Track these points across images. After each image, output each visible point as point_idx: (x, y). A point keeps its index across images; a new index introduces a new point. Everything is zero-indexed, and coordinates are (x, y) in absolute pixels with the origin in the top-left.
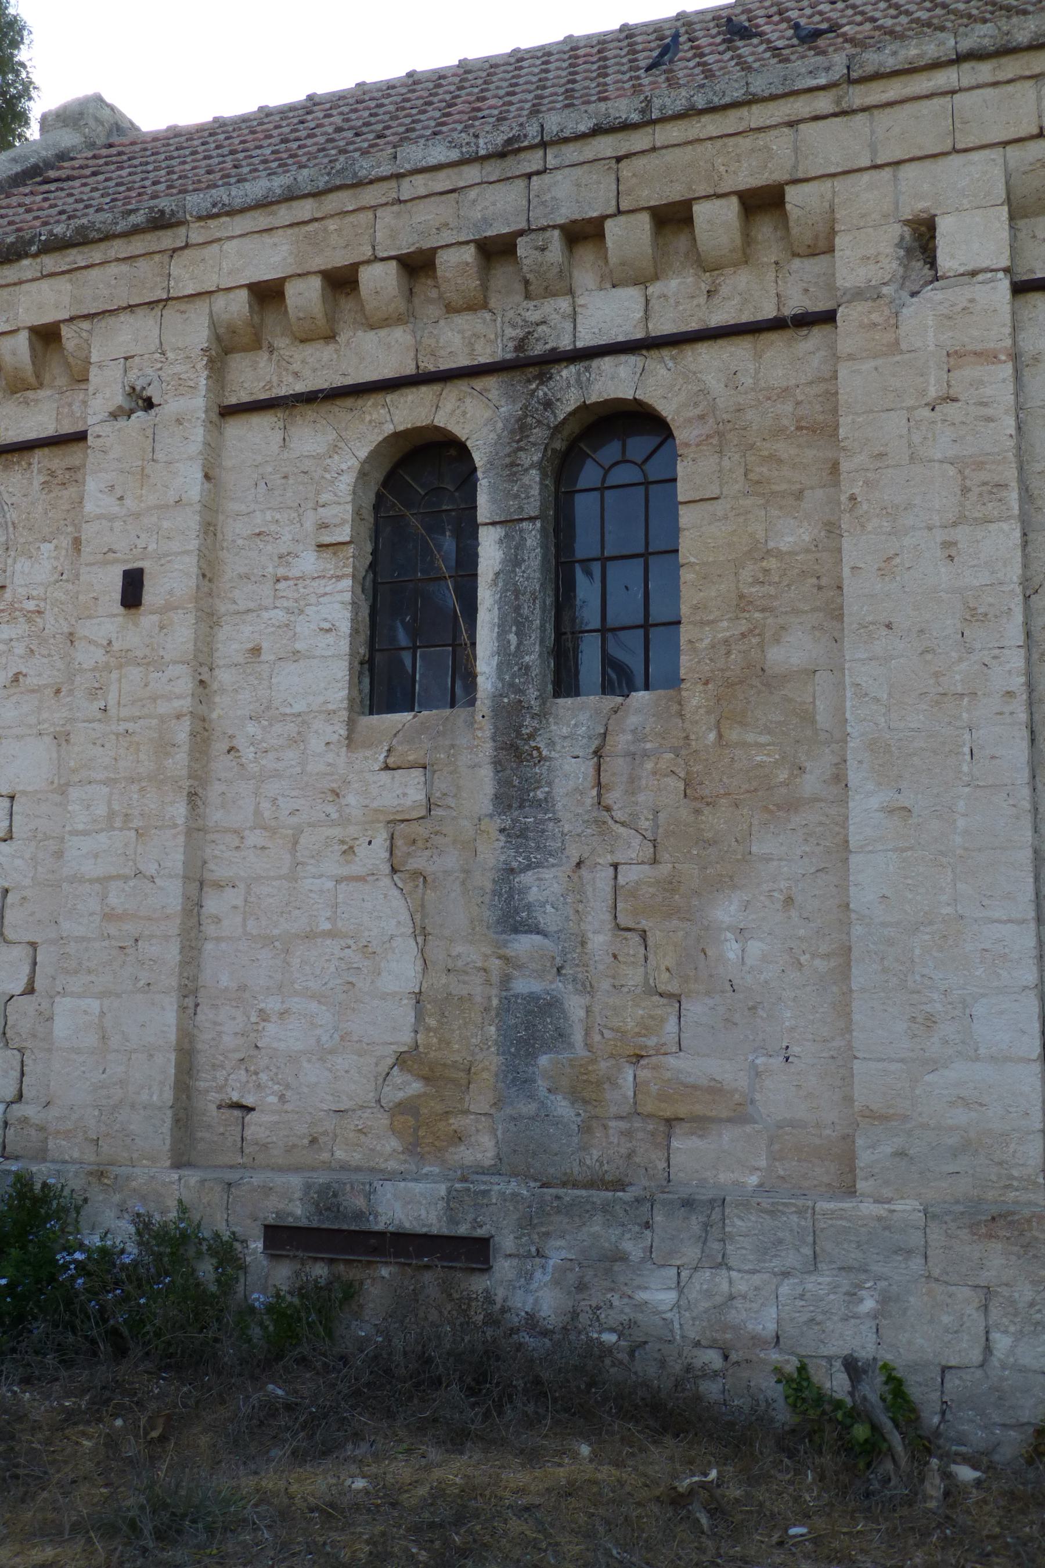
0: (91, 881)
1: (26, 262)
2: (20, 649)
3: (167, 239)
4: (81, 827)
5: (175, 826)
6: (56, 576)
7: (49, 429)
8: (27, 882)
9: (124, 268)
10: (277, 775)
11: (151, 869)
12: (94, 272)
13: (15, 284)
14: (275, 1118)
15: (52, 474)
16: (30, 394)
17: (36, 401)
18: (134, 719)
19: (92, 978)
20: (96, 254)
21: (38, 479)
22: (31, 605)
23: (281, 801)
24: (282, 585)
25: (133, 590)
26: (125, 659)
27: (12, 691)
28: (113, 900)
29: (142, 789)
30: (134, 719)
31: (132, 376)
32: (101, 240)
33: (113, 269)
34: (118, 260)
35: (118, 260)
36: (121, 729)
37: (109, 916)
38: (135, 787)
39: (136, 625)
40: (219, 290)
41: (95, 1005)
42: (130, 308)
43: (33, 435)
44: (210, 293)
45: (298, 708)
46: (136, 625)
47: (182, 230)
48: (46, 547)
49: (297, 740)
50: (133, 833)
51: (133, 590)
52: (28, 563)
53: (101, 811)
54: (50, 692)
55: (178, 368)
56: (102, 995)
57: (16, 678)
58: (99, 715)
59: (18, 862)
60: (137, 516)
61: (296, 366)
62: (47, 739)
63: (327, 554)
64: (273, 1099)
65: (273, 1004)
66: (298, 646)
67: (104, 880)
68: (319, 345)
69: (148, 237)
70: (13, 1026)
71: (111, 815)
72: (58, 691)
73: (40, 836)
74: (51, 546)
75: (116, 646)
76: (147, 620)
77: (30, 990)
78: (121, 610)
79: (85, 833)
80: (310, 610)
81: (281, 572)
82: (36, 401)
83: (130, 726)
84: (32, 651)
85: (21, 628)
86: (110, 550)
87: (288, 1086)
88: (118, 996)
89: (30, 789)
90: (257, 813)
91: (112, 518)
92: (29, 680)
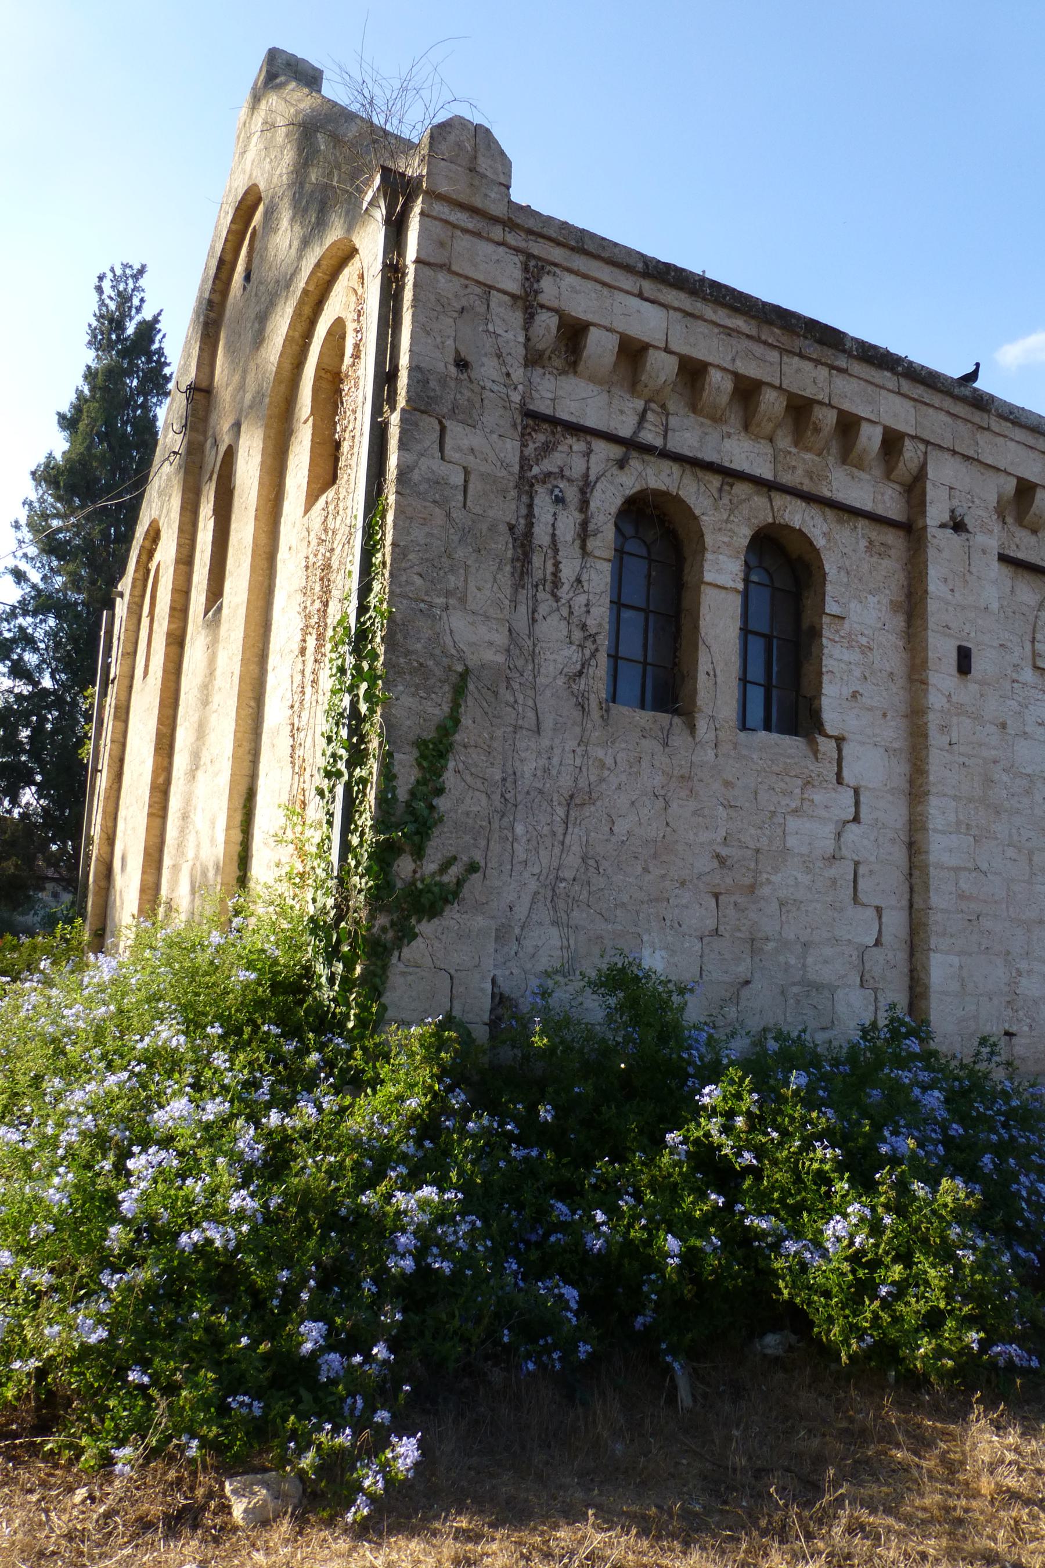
0: (952, 869)
1: (888, 374)
2: (857, 673)
3: (978, 417)
4: (940, 827)
5: (997, 839)
6: (880, 625)
7: (868, 507)
8: (873, 859)
9: (949, 420)
10: (1018, 812)
11: (984, 866)
12: (931, 410)
13: (877, 386)
14: (1028, 1041)
15: (871, 542)
16: (855, 470)
17: (860, 480)
18: (969, 756)
19: (953, 940)
20: (936, 399)
21: (863, 543)
22: (864, 641)
23: (1022, 830)
24: (1015, 685)
25: (964, 660)
26: (961, 710)
27: (853, 704)
28: (963, 885)
29: (976, 808)
30: (969, 756)
31: (956, 502)
32: (941, 391)
33: (943, 417)
34: (948, 412)
35: (948, 412)
36: (961, 760)
37: (962, 897)
38: (972, 806)
39: (966, 687)
40: (1005, 471)
41: (955, 960)
42: (954, 452)
43: (857, 505)
44: (998, 470)
45: (1029, 771)
46: (966, 687)
47: (986, 416)
48: (870, 597)
49: (1028, 792)
50: (971, 839)
51: (964, 660)
52: (859, 606)
53: (952, 818)
54: (879, 713)
55: (980, 513)
56: (960, 953)
57: (855, 695)
58: (947, 747)
59: (866, 842)
60: (964, 608)
61: (1017, 540)
62: (882, 750)
63: (1038, 673)
64: (1026, 1028)
65: (1023, 965)
66: (1027, 729)
67: (957, 870)
68: (1029, 533)
69: (967, 408)
70: (870, 971)
71: (958, 823)
72: (885, 715)
73: (880, 825)
74: (875, 600)
75: (954, 699)
76: (973, 687)
77: (878, 943)
78: (953, 670)
79: (943, 832)
80: (1031, 707)
81: (1015, 676)
82: (860, 480)
83: (966, 760)
84: (865, 678)
85: (854, 656)
86: (947, 626)
87: (1034, 1020)
88: (970, 955)
89: (870, 786)
90: (1010, 835)
91: (948, 603)
92: (864, 700)
